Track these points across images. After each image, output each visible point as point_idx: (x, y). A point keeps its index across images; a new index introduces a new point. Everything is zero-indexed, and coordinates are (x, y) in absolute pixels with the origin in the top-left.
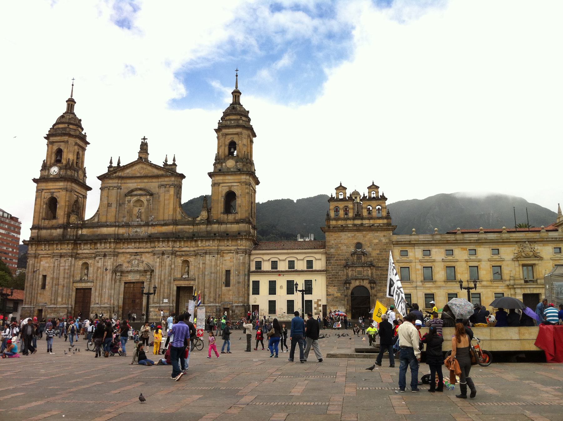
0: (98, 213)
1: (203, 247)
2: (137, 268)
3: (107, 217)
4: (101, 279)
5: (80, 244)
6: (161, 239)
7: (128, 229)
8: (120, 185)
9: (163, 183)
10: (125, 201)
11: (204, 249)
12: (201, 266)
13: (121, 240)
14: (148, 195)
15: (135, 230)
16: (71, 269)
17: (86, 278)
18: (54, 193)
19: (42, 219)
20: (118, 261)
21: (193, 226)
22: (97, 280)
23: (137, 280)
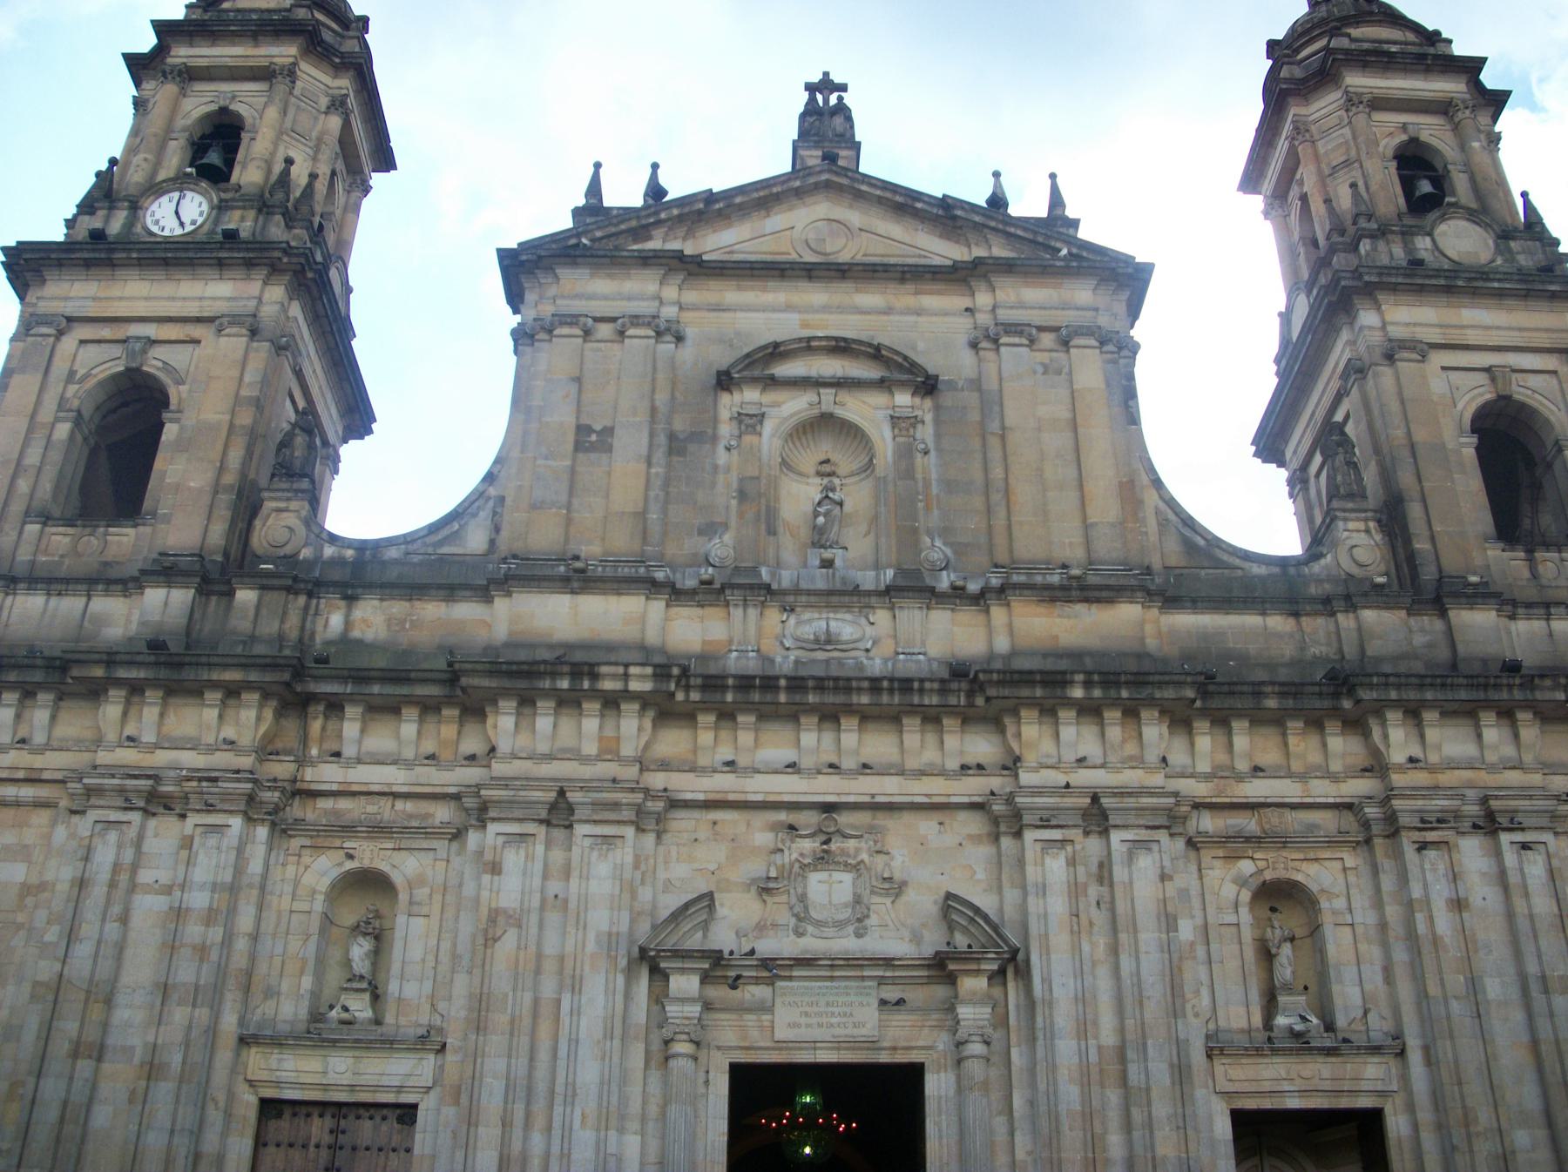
0: (492, 491)
1: (1432, 769)
2: (846, 944)
3: (569, 521)
4: (527, 1022)
5: (335, 707)
6: (1078, 693)
7: (753, 612)
8: (669, 312)
9: (1003, 315)
10: (715, 421)
11: (1436, 787)
12: (1444, 922)
13: (713, 683)
14: (902, 384)
15: (811, 623)
16: (232, 911)
17: (360, 1007)
18: (158, 352)
19: (27, 516)
20: (662, 875)
21: (1296, 615)
22: (479, 1025)
23: (853, 1044)
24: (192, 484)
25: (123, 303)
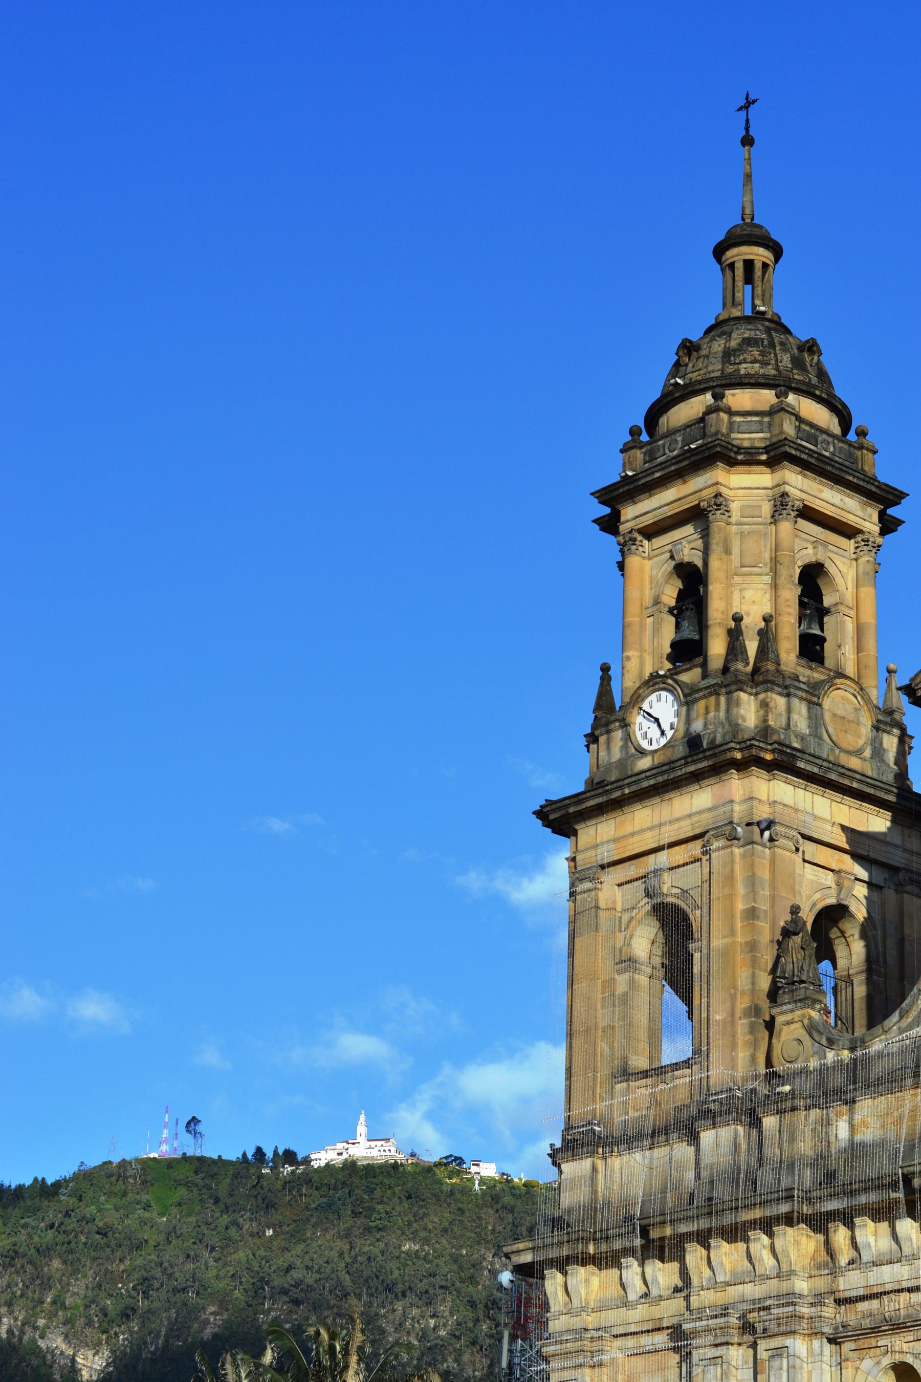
24: (718, 1017)
25: (636, 838)
